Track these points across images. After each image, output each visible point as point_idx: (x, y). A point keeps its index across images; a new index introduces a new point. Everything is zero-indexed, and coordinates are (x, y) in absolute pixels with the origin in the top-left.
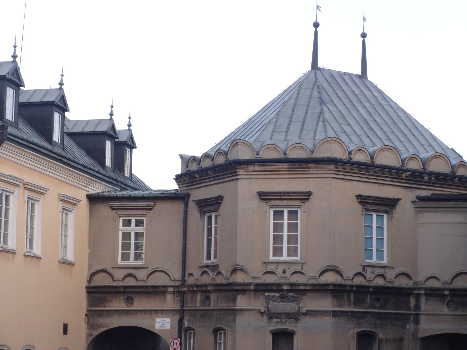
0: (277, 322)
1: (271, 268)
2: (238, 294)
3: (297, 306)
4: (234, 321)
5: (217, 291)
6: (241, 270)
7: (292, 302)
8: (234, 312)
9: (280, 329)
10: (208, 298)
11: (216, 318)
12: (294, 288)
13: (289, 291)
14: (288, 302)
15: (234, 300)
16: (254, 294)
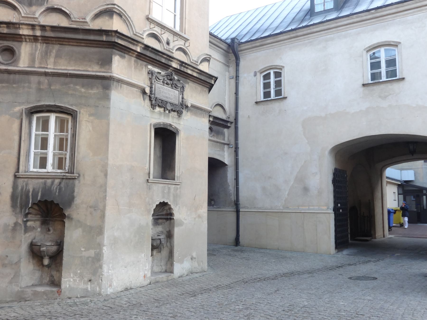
0: (160, 113)
1: (157, 30)
2: (116, 54)
3: (181, 96)
4: (107, 98)
5: (46, 40)
6: (120, 15)
7: (176, 87)
8: (106, 82)
9: (164, 124)
10: (11, 51)
11: (39, 90)
12: (182, 69)
13: (176, 71)
14: (172, 87)
15: (107, 62)
16: (135, 61)
